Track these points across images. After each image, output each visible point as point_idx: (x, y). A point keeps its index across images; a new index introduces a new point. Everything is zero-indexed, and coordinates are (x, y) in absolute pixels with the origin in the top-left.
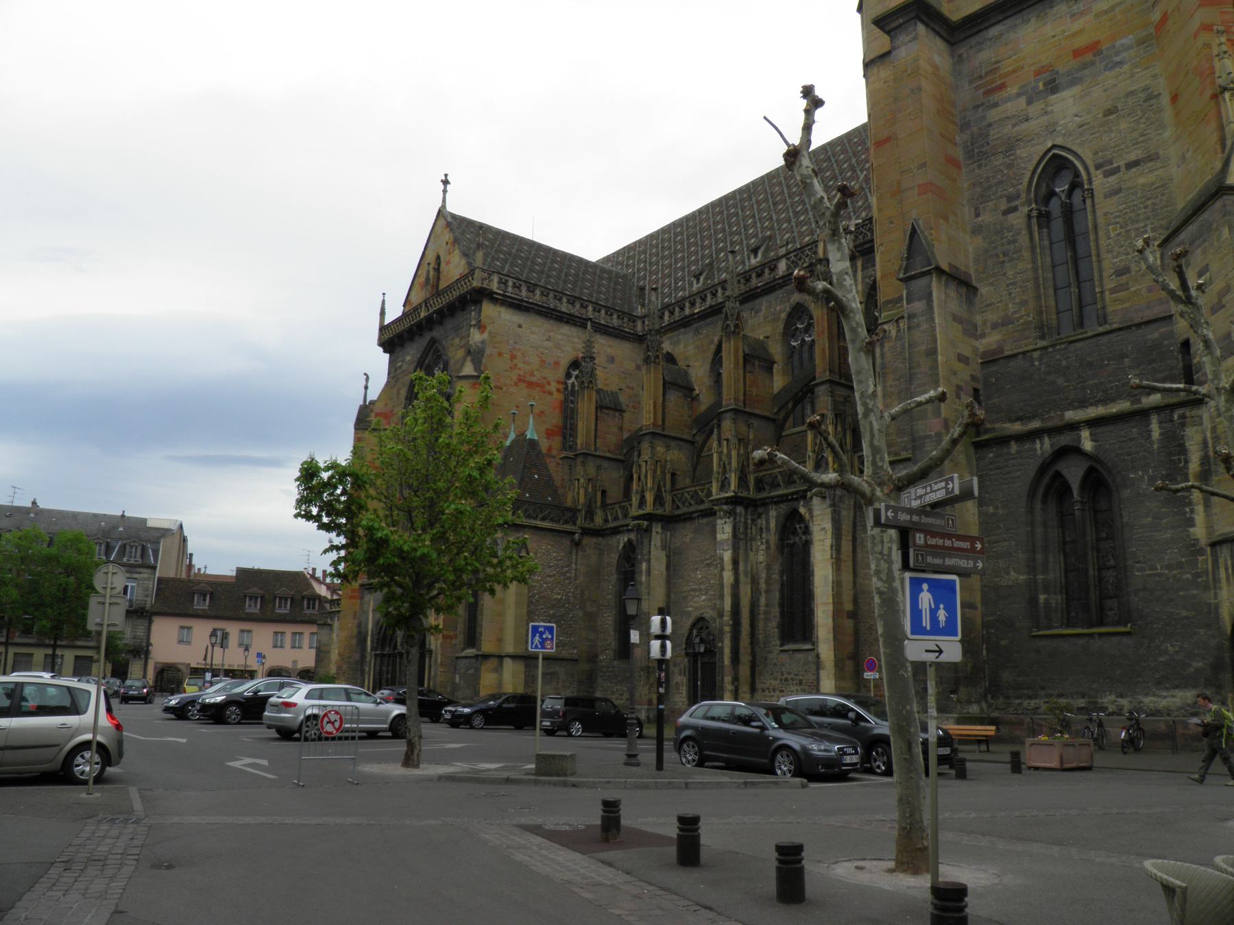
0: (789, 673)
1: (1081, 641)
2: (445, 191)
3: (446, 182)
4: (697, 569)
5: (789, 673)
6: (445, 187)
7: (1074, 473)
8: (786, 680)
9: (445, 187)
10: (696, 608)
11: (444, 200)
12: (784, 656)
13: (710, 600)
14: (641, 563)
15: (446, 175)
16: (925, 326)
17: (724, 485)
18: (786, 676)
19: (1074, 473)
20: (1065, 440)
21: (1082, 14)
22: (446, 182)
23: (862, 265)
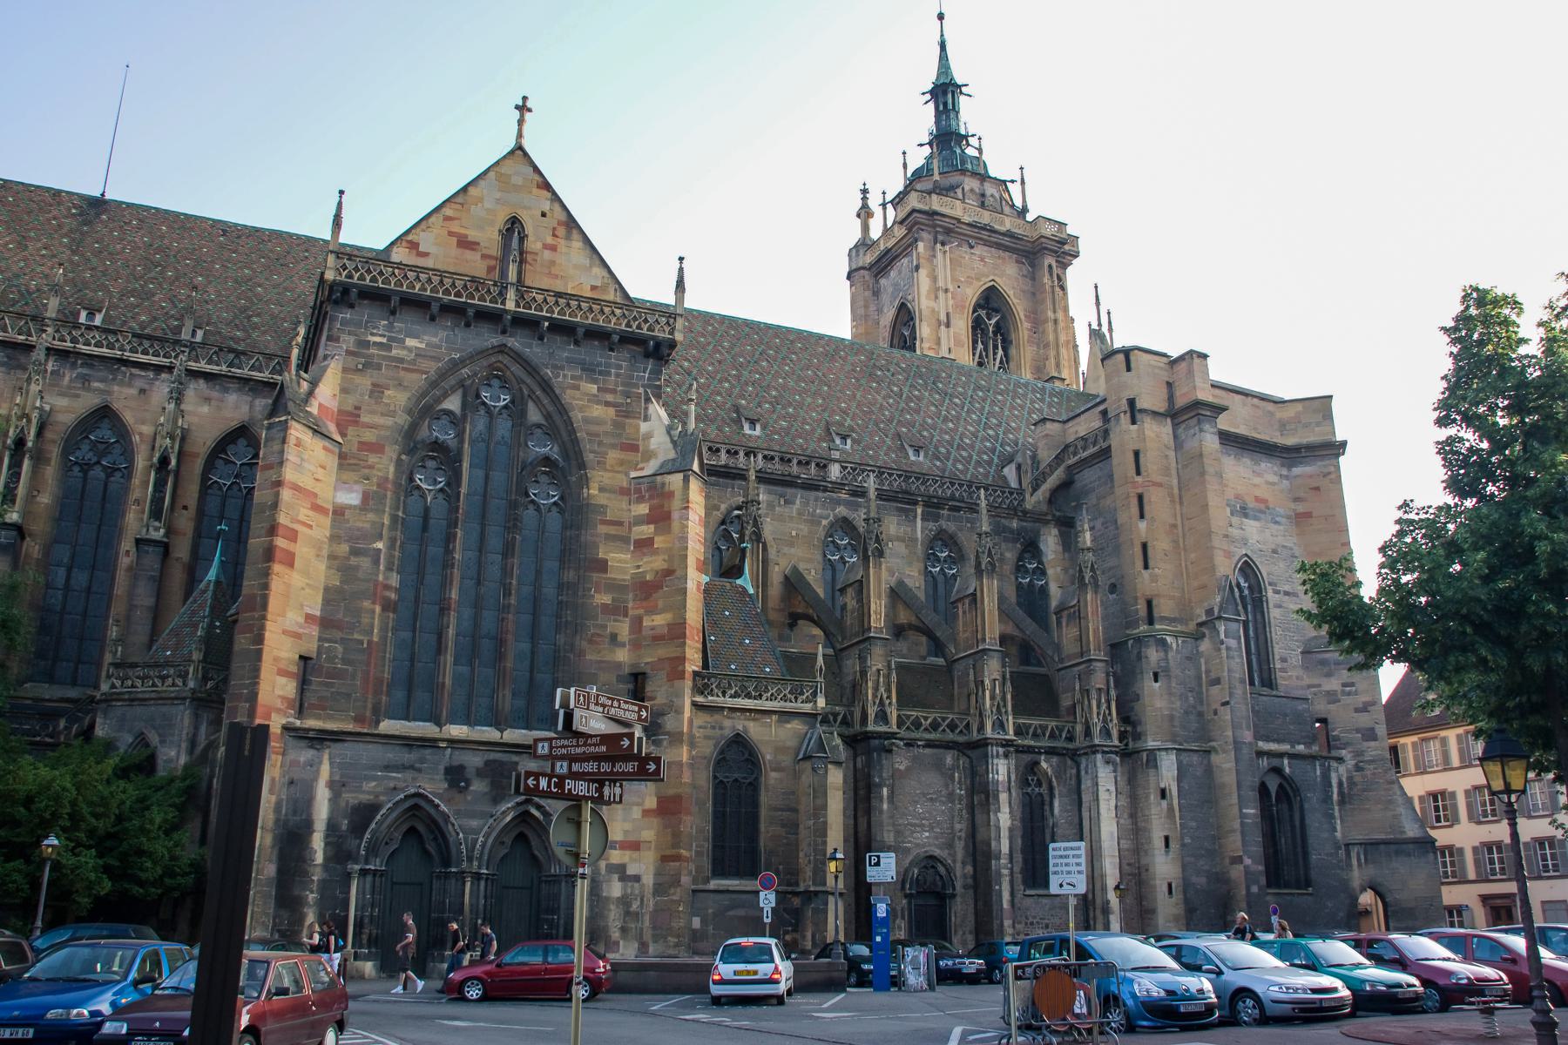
0: (1034, 917)
1: (1289, 898)
2: (521, 122)
3: (523, 108)
4: (917, 802)
5: (1034, 917)
6: (522, 116)
7: (1273, 785)
8: (1032, 924)
9: (522, 116)
10: (917, 845)
11: (520, 135)
12: (1029, 901)
13: (936, 838)
14: (880, 786)
15: (525, 98)
16: (1238, 660)
17: (1000, 725)
18: (1031, 920)
19: (1273, 785)
20: (1275, 762)
21: (1259, 475)
22: (523, 108)
23: (922, 515)
